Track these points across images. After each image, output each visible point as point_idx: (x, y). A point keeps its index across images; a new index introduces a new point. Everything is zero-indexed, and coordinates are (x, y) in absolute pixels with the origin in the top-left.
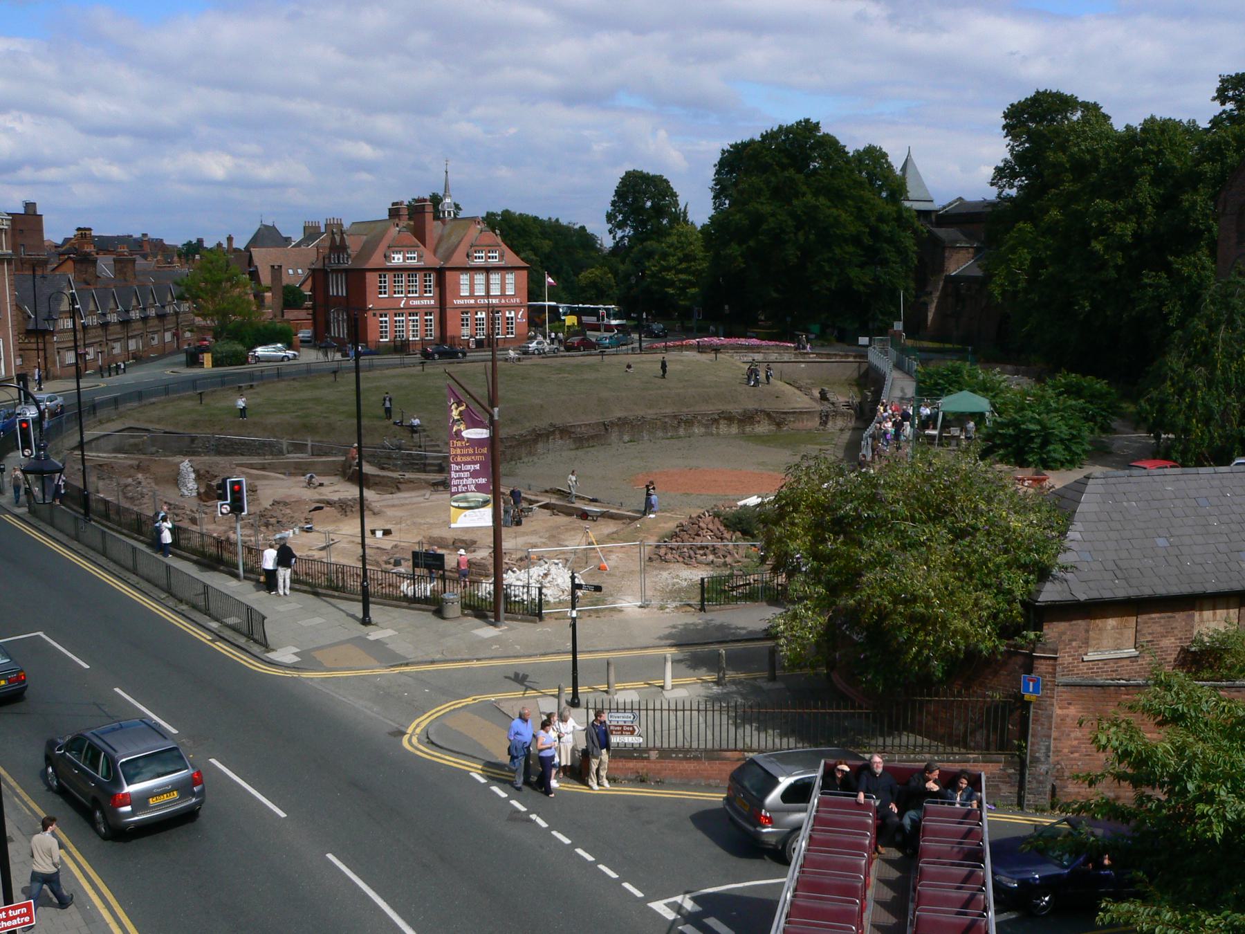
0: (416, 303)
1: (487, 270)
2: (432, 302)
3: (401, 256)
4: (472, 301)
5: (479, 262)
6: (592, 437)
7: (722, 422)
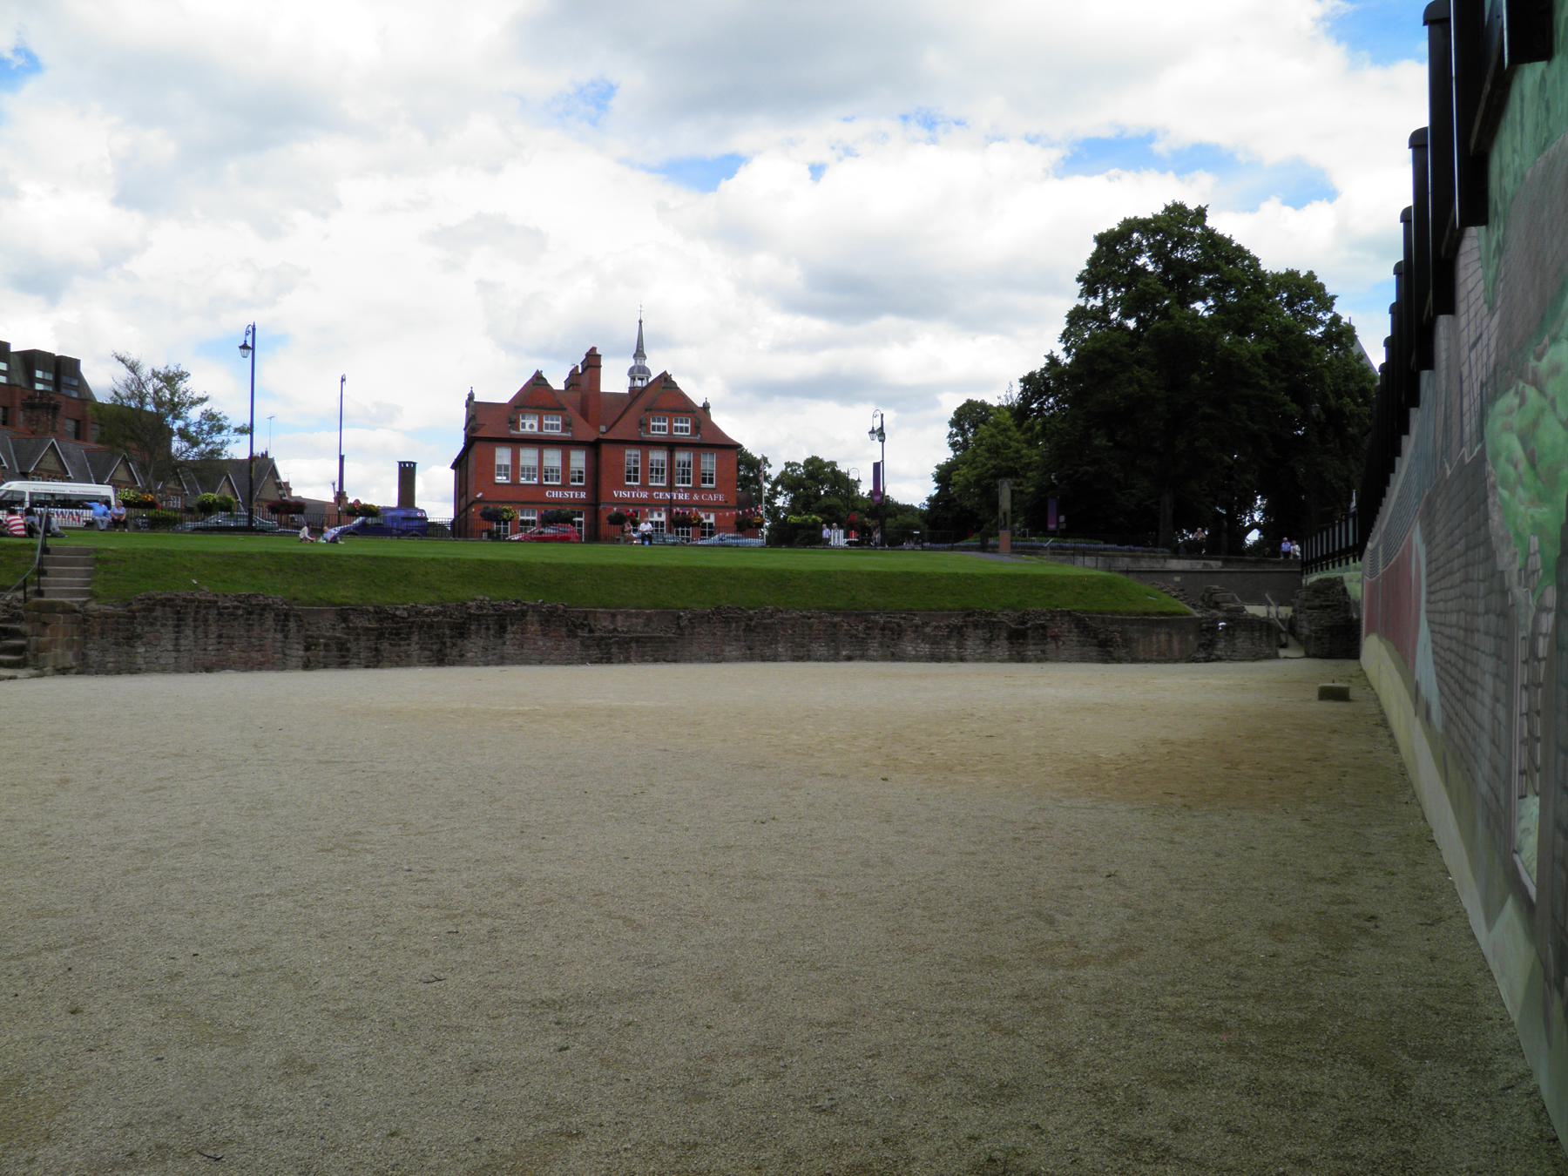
0: (556, 494)
1: (671, 446)
2: (583, 495)
4: (644, 495)
5: (656, 434)
6: (637, 640)
7: (969, 631)
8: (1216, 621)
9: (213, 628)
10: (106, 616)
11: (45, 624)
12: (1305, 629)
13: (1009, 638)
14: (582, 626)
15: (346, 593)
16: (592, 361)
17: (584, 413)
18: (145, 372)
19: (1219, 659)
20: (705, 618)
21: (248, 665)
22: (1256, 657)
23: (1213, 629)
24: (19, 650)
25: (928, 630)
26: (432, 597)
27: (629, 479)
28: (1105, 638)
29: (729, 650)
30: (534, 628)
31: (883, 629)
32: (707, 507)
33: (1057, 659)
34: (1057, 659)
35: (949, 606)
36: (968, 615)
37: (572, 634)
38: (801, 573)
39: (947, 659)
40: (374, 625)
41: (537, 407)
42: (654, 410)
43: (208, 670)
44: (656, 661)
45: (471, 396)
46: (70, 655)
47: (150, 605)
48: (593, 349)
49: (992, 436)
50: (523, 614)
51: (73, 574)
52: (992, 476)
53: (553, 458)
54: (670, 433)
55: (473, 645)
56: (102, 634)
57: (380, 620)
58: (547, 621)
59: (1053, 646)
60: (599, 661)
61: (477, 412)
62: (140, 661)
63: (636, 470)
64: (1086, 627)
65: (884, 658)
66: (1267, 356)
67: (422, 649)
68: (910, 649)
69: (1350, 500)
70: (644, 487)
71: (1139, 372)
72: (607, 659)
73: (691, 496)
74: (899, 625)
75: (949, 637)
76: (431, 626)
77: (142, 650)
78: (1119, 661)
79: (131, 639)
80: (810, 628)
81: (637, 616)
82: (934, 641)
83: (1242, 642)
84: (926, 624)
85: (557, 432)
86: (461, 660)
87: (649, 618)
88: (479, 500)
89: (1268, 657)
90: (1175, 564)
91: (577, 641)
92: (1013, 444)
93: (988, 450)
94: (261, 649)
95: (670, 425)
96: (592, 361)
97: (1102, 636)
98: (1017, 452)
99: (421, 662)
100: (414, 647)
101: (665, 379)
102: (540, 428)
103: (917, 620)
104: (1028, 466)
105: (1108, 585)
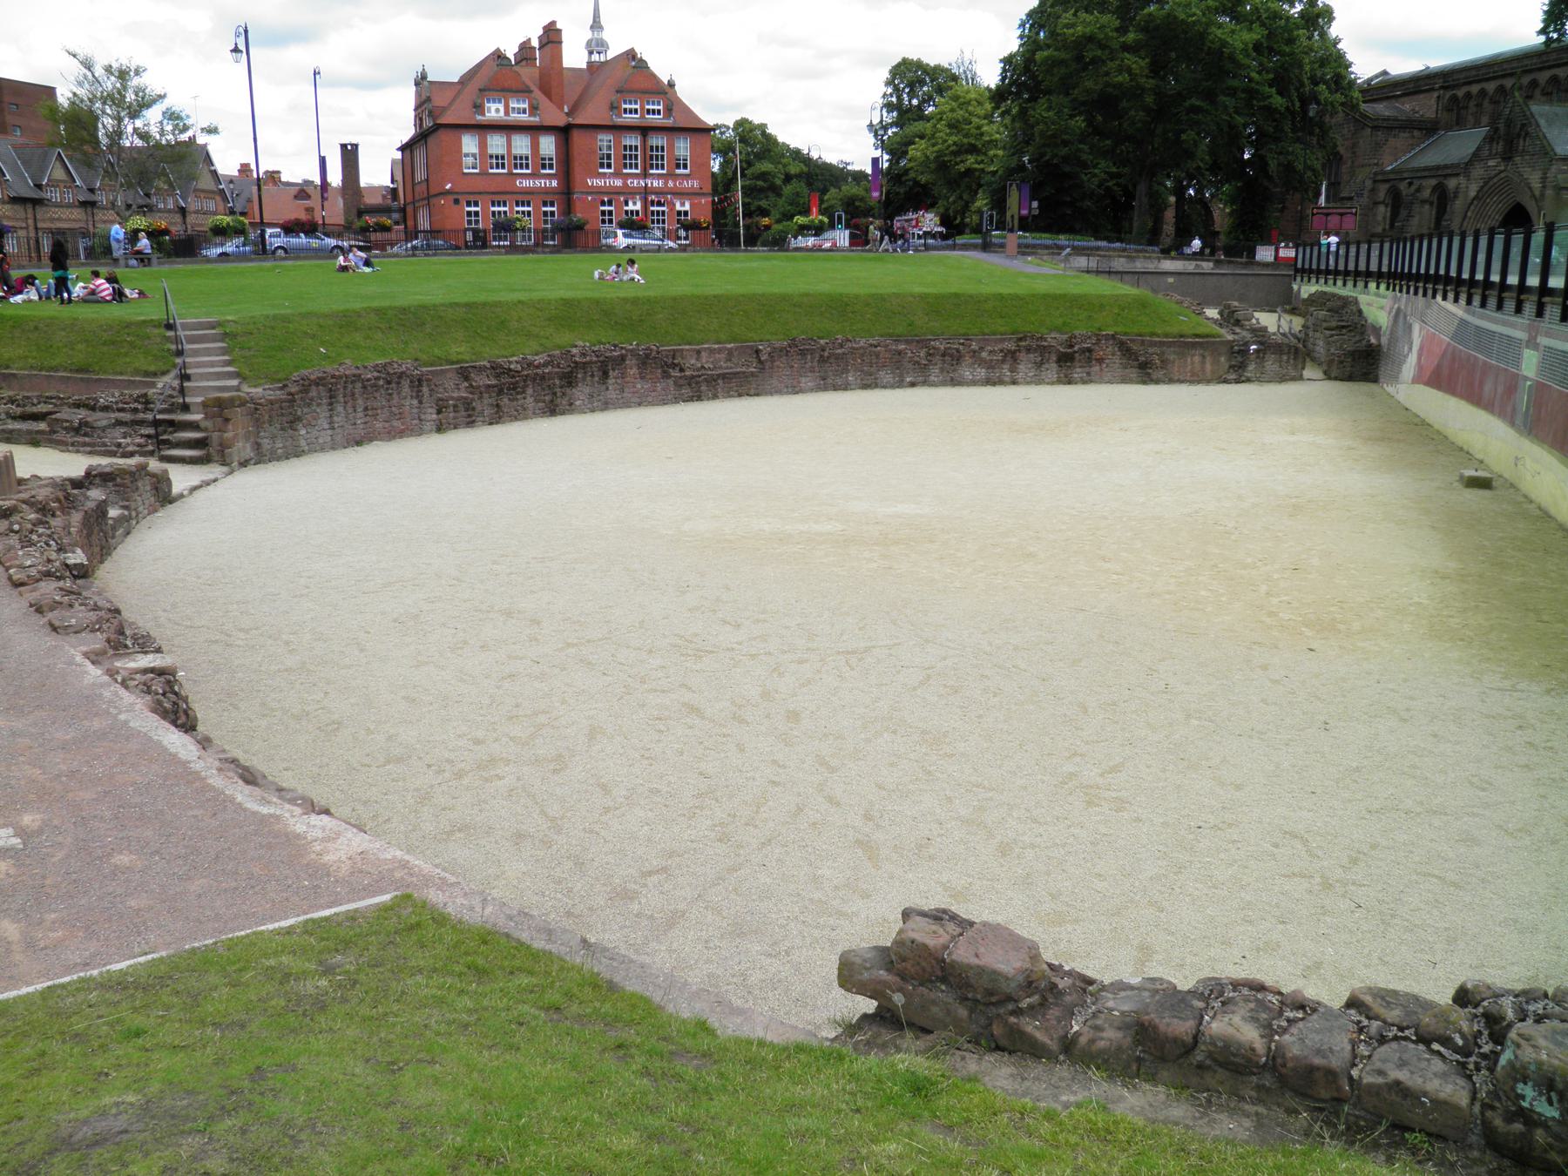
0: (527, 183)
1: (645, 131)
2: (554, 183)
3: (501, 107)
4: (618, 183)
5: (628, 118)
6: (724, 376)
7: (1022, 356)
8: (1247, 344)
9: (360, 401)
10: (271, 402)
11: (227, 420)
12: (1320, 348)
13: (1058, 361)
14: (674, 366)
15: (459, 349)
16: (551, 36)
17: (547, 92)
18: (99, 71)
19: (1248, 380)
20: (784, 351)
21: (393, 434)
22: (1282, 379)
23: (1244, 352)
24: (199, 444)
25: (984, 354)
26: (534, 345)
27: (602, 165)
28: (1144, 360)
29: (806, 381)
30: (633, 371)
31: (943, 355)
32: (681, 194)
33: (1101, 381)
34: (1101, 381)
35: (1002, 329)
36: (1020, 339)
37: (666, 375)
38: (857, 297)
39: (1000, 382)
40: (494, 382)
41: (503, 90)
42: (624, 91)
43: (359, 443)
44: (740, 395)
45: (424, 77)
46: (249, 449)
47: (307, 385)
48: (553, 23)
49: (952, 110)
50: (623, 358)
51: (208, 352)
52: (953, 153)
53: (521, 145)
54: (642, 117)
55: (581, 393)
56: (270, 423)
57: (497, 376)
58: (644, 363)
59: (1097, 368)
60: (690, 399)
61: (429, 95)
62: (303, 443)
63: (609, 157)
64: (1128, 350)
65: (943, 384)
66: (1257, 47)
67: (537, 401)
68: (967, 374)
69: (1318, 195)
70: (617, 174)
71: (1130, 59)
72: (699, 398)
73: (666, 183)
74: (958, 351)
75: (1003, 361)
76: (543, 378)
77: (303, 432)
78: (1157, 382)
79: (294, 422)
80: (877, 356)
81: (720, 351)
82: (990, 366)
83: (1271, 364)
84: (982, 349)
85: (524, 118)
86: (570, 409)
87: (730, 352)
88: (449, 192)
89: (1293, 379)
90: (1168, 265)
91: (671, 382)
92: (975, 120)
93: (950, 126)
94: (401, 416)
95: (642, 108)
96: (551, 36)
97: (1142, 359)
98: (979, 128)
99: (535, 415)
100: (530, 400)
101: (631, 55)
102: (507, 113)
103: (974, 346)
104: (993, 143)
105: (1143, 304)
